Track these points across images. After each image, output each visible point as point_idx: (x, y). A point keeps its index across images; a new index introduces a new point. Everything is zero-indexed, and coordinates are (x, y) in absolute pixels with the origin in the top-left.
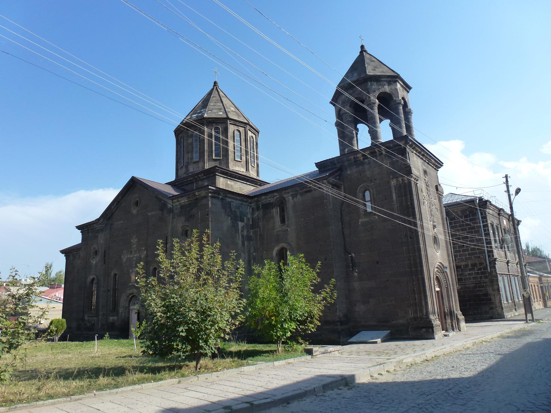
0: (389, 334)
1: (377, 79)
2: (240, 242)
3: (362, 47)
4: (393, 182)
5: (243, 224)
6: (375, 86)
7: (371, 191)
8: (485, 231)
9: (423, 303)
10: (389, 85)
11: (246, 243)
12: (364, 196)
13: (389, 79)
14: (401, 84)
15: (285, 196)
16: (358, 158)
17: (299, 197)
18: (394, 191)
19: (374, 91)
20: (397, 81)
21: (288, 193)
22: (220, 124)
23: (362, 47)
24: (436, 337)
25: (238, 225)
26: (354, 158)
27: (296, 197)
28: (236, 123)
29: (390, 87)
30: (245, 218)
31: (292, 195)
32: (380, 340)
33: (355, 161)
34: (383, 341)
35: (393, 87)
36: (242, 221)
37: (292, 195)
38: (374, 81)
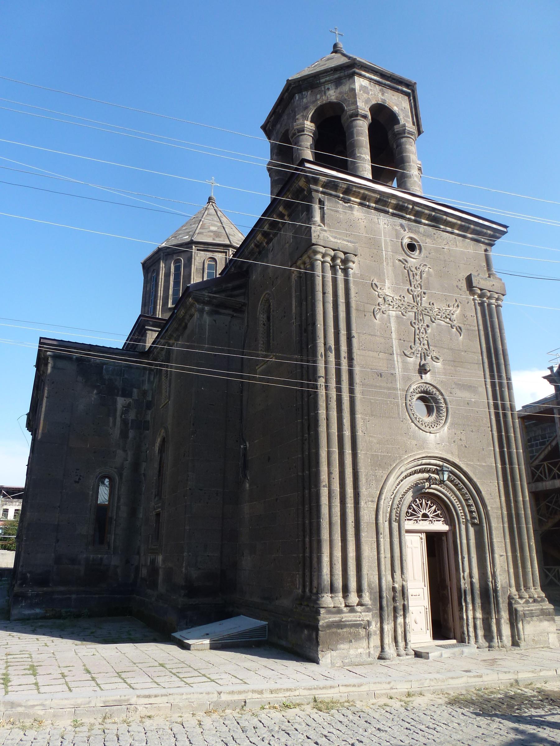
0: (176, 631)
2: (116, 432)
5: (129, 400)
6: (308, 97)
9: (315, 560)
10: (337, 87)
11: (131, 434)
13: (336, 76)
14: (370, 80)
19: (306, 108)
20: (354, 74)
22: (182, 254)
23: (335, 46)
24: (326, 657)
25: (115, 402)
28: (206, 246)
29: (338, 90)
30: (135, 390)
32: (207, 642)
33: (260, 253)
34: (214, 647)
35: (345, 88)
36: (126, 394)
38: (306, 90)
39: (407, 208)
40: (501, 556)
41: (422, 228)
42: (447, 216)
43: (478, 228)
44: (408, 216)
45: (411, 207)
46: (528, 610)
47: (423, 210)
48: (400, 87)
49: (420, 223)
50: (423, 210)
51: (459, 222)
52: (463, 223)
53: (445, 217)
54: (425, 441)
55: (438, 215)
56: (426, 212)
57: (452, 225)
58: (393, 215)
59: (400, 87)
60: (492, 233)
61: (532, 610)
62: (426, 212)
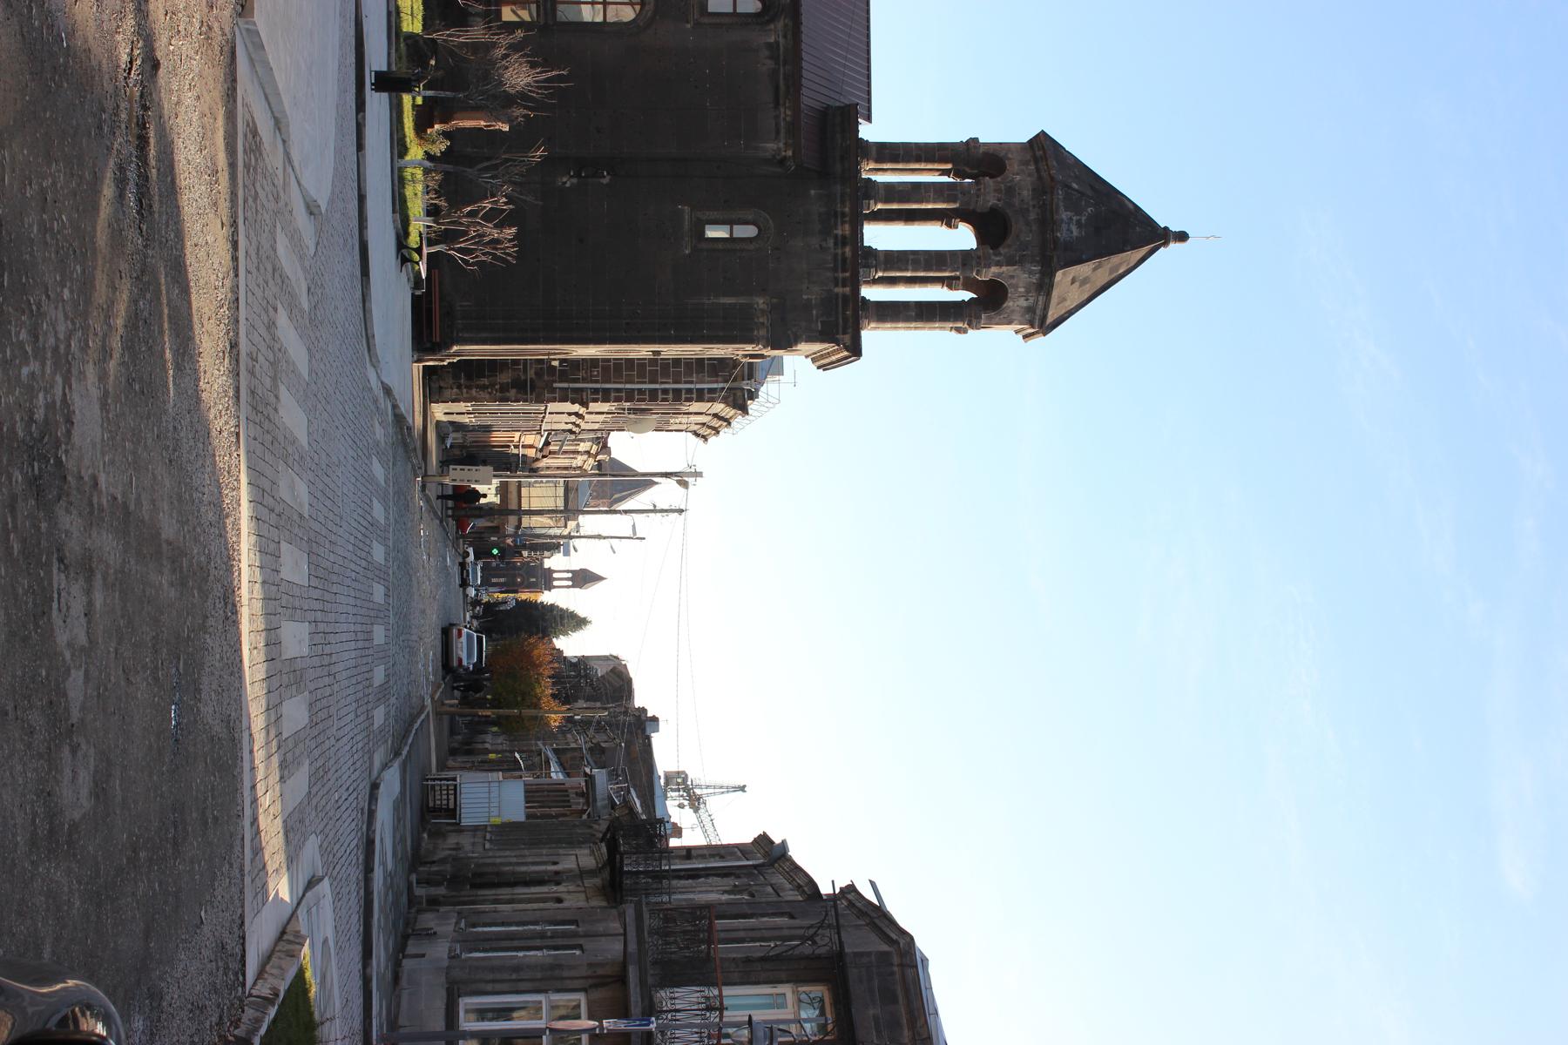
1: (1045, 286)
3: (1182, 237)
4: (760, 302)
7: (752, 247)
8: (665, 391)
9: (484, 335)
12: (746, 223)
15: (780, 24)
16: (843, 223)
17: (770, 64)
18: (742, 300)
21: (785, 37)
26: (843, 215)
27: (771, 58)
31: (777, 43)
37: (777, 43)
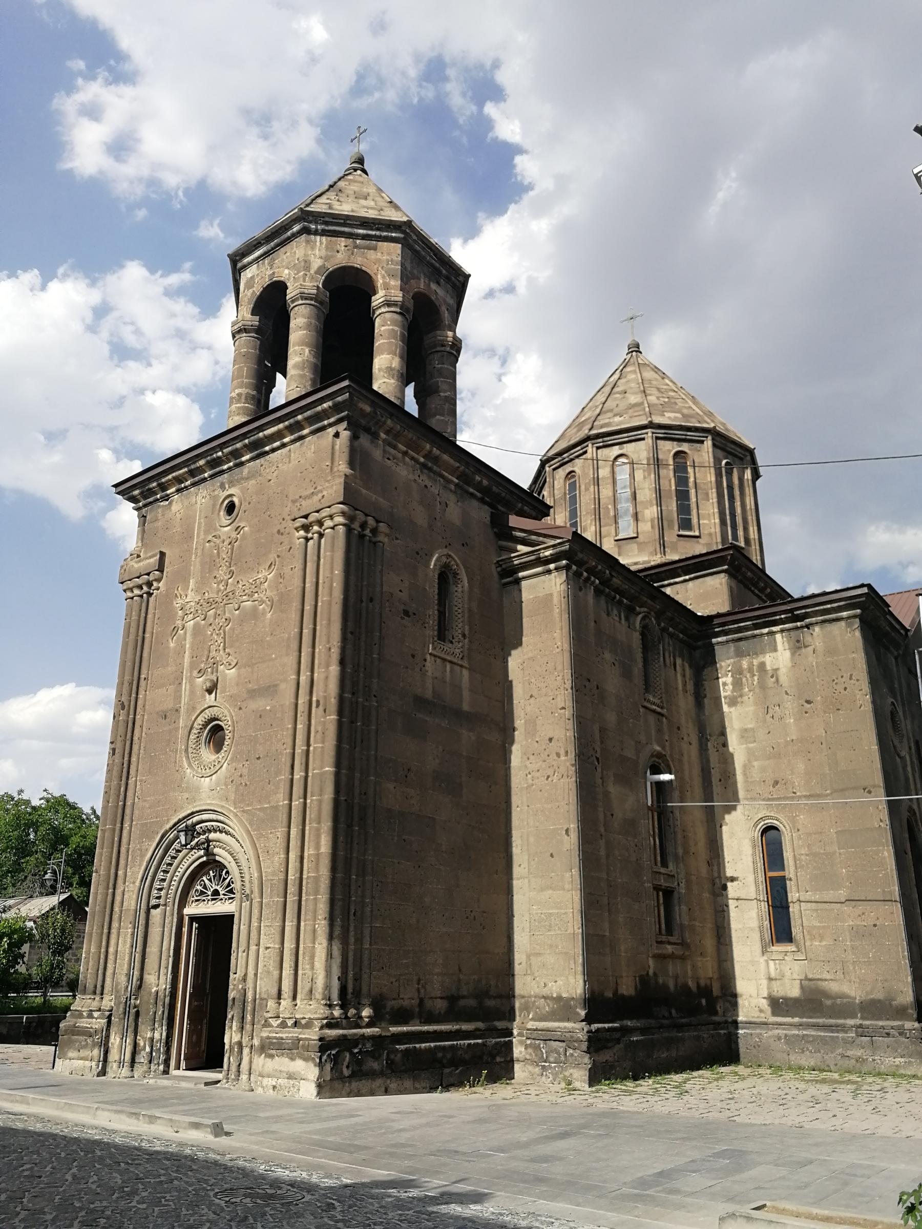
39: (219, 458)
40: (267, 948)
41: (245, 470)
42: (263, 431)
43: (309, 413)
44: (225, 467)
45: (220, 454)
46: (275, 1038)
47: (234, 447)
48: (289, 233)
49: (242, 464)
50: (234, 447)
51: (281, 426)
52: (287, 423)
53: (261, 434)
54: (197, 789)
55: (252, 438)
56: (239, 445)
57: (279, 435)
58: (212, 477)
59: (289, 233)
60: (330, 403)
61: (282, 1039)
62: (239, 445)
